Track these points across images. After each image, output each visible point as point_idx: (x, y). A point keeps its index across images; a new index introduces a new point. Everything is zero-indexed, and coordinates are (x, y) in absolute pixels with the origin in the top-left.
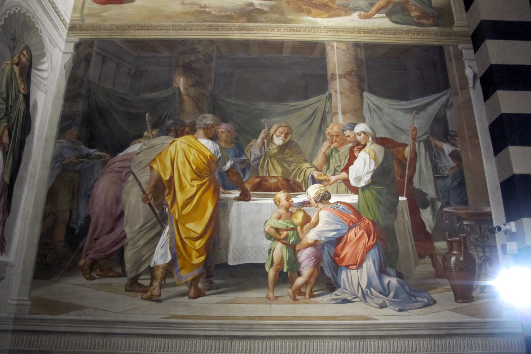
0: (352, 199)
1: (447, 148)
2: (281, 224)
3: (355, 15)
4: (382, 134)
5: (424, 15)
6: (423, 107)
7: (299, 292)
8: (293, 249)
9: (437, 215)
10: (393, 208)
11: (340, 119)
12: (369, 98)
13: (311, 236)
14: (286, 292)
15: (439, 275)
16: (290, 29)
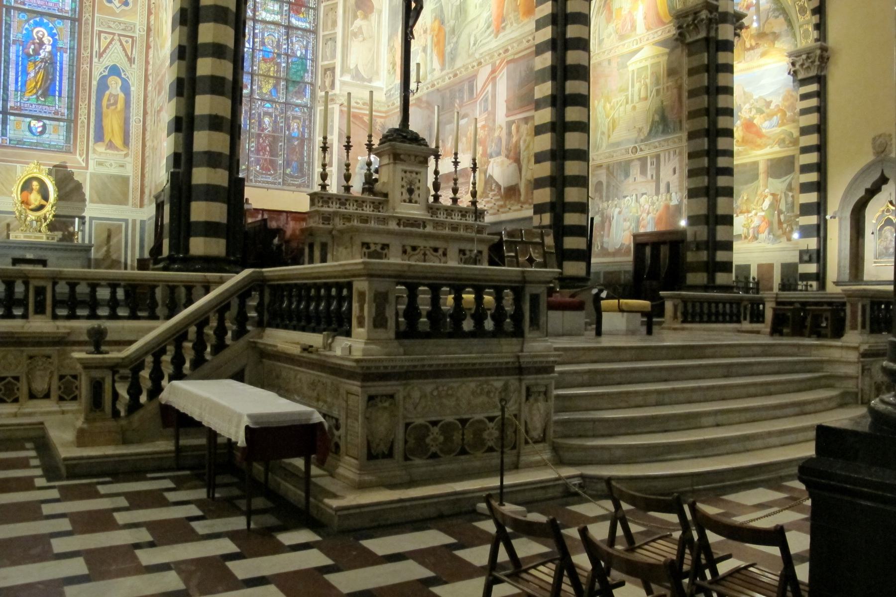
0: (763, 214)
1: (790, 194)
2: (746, 223)
3: (768, 147)
4: (773, 192)
5: (791, 142)
6: (784, 181)
7: (749, 241)
8: (748, 229)
9: (785, 216)
10: (773, 215)
11: (761, 188)
12: (770, 179)
13: (752, 225)
14: (747, 241)
15: (783, 234)
16: (749, 157)
